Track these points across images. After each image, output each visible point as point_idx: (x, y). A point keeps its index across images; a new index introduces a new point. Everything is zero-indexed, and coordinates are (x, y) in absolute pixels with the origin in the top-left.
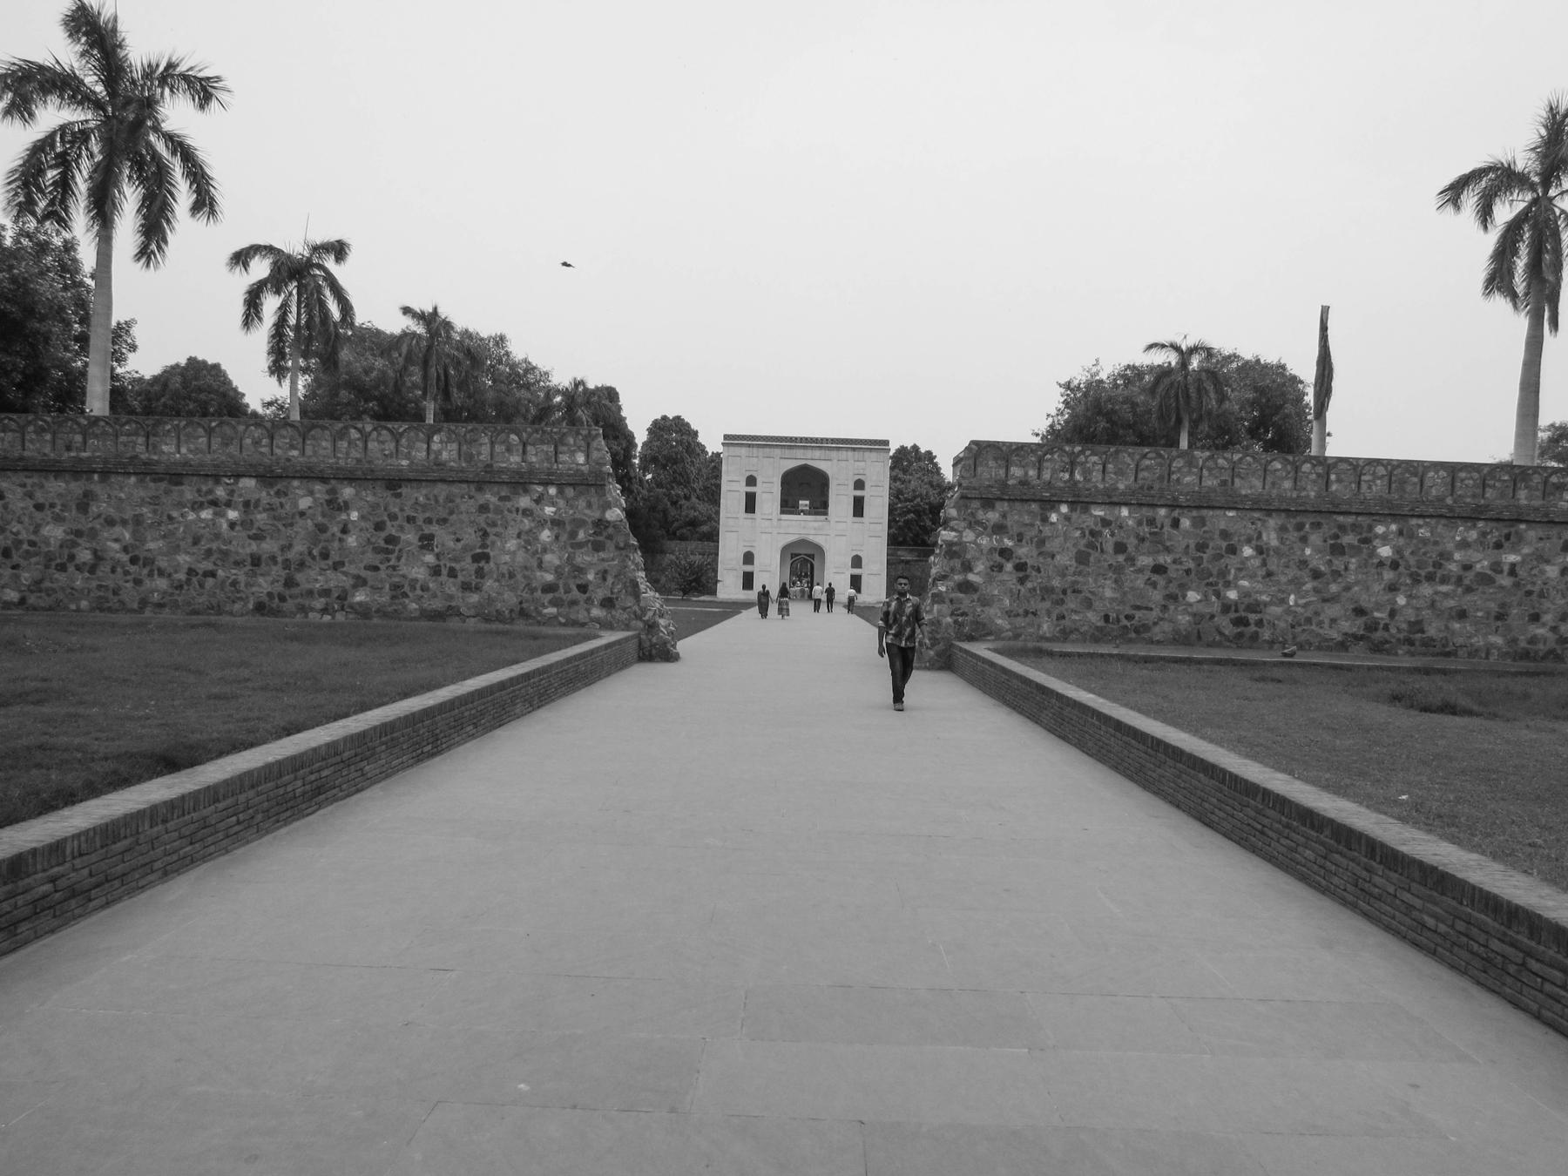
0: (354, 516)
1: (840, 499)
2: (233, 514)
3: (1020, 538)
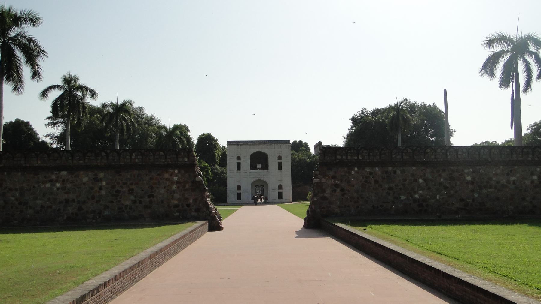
0: (104, 183)
1: (273, 164)
2: (58, 185)
3: (341, 180)
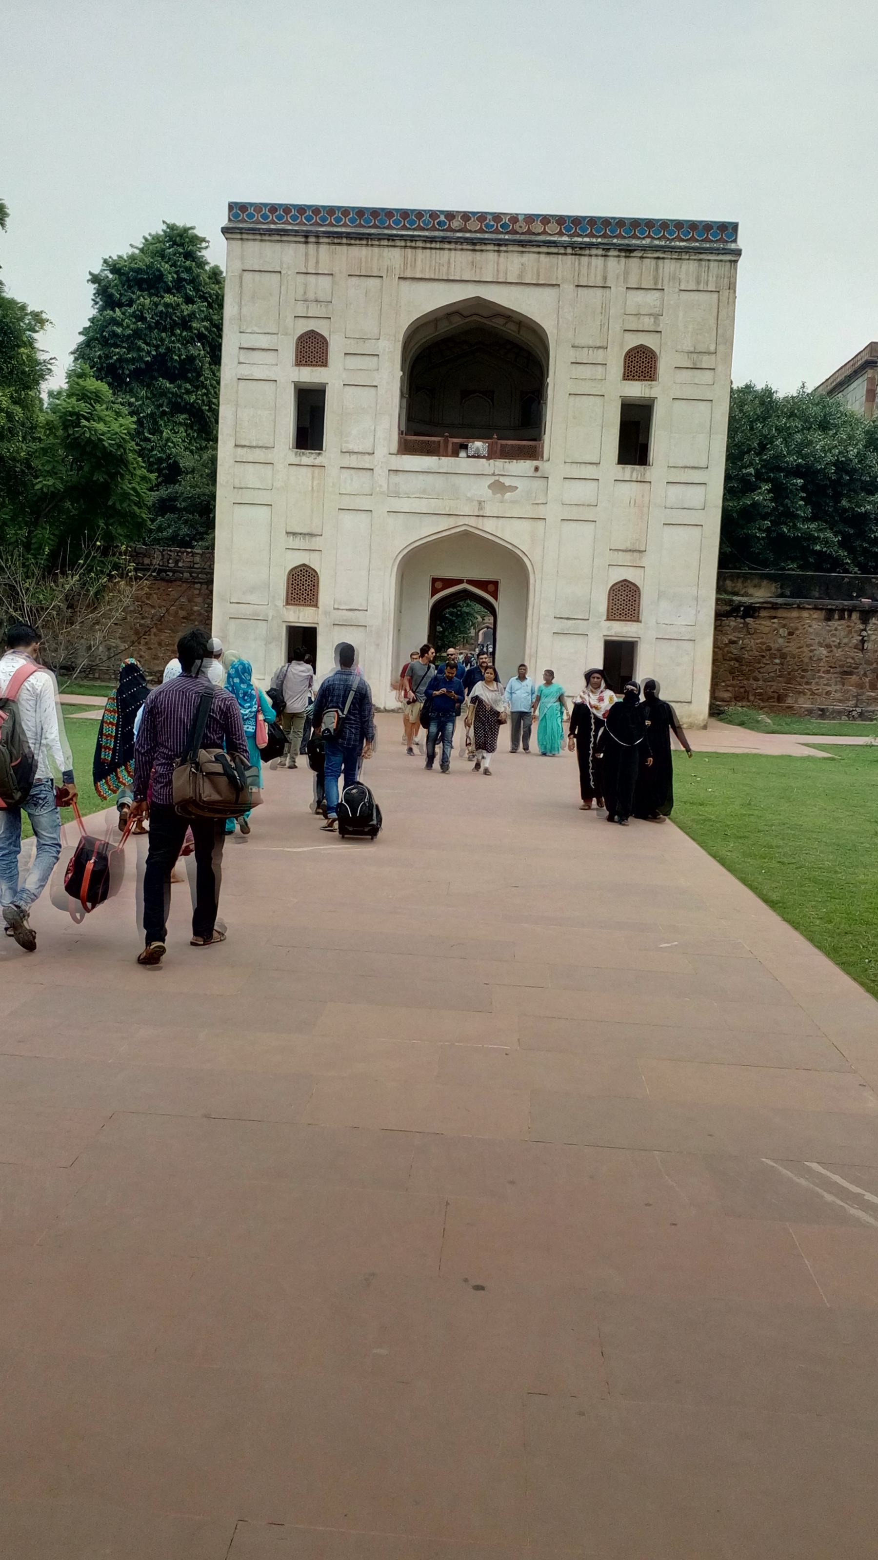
1: (578, 411)
